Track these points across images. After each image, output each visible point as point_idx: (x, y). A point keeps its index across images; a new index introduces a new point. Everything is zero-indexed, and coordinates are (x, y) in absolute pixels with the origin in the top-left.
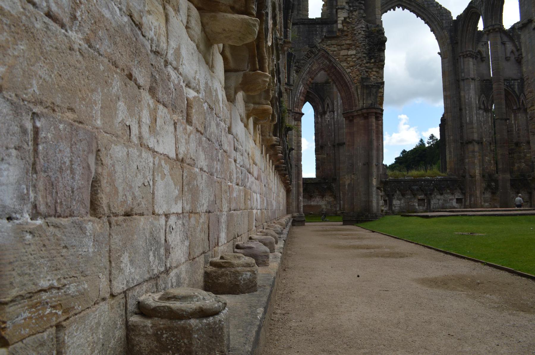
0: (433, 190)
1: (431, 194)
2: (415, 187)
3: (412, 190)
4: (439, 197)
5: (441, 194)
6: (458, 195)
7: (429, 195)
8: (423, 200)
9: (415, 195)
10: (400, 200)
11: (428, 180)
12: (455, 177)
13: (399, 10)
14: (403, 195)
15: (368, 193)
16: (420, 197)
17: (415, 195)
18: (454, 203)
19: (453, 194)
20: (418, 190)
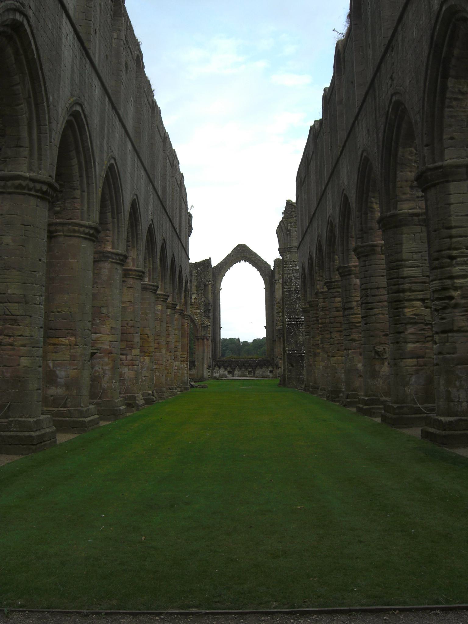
0: (257, 366)
1: (255, 368)
2: (247, 364)
3: (245, 366)
4: (260, 370)
5: (261, 368)
6: (270, 369)
7: (254, 369)
8: (251, 371)
9: (247, 369)
10: (238, 371)
11: (254, 361)
12: (269, 359)
13: (243, 262)
14: (240, 369)
15: (203, 371)
16: (250, 370)
17: (247, 369)
18: (268, 373)
19: (268, 368)
20: (248, 366)
